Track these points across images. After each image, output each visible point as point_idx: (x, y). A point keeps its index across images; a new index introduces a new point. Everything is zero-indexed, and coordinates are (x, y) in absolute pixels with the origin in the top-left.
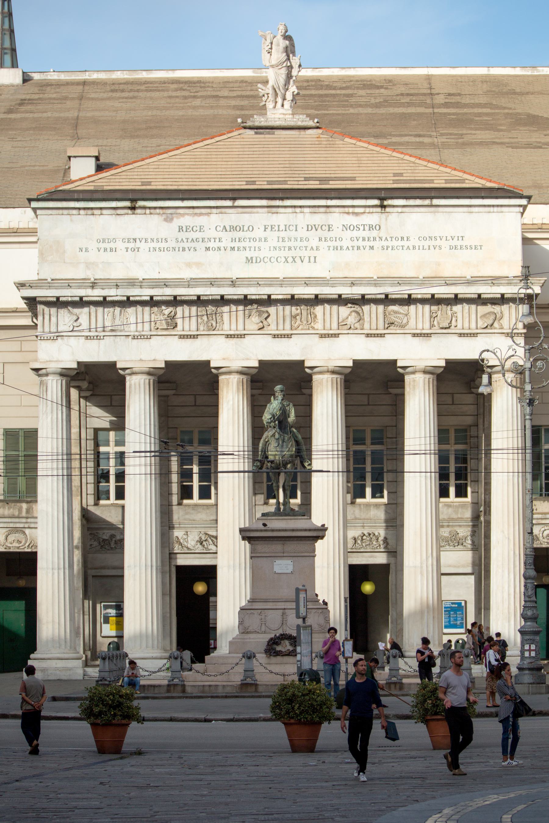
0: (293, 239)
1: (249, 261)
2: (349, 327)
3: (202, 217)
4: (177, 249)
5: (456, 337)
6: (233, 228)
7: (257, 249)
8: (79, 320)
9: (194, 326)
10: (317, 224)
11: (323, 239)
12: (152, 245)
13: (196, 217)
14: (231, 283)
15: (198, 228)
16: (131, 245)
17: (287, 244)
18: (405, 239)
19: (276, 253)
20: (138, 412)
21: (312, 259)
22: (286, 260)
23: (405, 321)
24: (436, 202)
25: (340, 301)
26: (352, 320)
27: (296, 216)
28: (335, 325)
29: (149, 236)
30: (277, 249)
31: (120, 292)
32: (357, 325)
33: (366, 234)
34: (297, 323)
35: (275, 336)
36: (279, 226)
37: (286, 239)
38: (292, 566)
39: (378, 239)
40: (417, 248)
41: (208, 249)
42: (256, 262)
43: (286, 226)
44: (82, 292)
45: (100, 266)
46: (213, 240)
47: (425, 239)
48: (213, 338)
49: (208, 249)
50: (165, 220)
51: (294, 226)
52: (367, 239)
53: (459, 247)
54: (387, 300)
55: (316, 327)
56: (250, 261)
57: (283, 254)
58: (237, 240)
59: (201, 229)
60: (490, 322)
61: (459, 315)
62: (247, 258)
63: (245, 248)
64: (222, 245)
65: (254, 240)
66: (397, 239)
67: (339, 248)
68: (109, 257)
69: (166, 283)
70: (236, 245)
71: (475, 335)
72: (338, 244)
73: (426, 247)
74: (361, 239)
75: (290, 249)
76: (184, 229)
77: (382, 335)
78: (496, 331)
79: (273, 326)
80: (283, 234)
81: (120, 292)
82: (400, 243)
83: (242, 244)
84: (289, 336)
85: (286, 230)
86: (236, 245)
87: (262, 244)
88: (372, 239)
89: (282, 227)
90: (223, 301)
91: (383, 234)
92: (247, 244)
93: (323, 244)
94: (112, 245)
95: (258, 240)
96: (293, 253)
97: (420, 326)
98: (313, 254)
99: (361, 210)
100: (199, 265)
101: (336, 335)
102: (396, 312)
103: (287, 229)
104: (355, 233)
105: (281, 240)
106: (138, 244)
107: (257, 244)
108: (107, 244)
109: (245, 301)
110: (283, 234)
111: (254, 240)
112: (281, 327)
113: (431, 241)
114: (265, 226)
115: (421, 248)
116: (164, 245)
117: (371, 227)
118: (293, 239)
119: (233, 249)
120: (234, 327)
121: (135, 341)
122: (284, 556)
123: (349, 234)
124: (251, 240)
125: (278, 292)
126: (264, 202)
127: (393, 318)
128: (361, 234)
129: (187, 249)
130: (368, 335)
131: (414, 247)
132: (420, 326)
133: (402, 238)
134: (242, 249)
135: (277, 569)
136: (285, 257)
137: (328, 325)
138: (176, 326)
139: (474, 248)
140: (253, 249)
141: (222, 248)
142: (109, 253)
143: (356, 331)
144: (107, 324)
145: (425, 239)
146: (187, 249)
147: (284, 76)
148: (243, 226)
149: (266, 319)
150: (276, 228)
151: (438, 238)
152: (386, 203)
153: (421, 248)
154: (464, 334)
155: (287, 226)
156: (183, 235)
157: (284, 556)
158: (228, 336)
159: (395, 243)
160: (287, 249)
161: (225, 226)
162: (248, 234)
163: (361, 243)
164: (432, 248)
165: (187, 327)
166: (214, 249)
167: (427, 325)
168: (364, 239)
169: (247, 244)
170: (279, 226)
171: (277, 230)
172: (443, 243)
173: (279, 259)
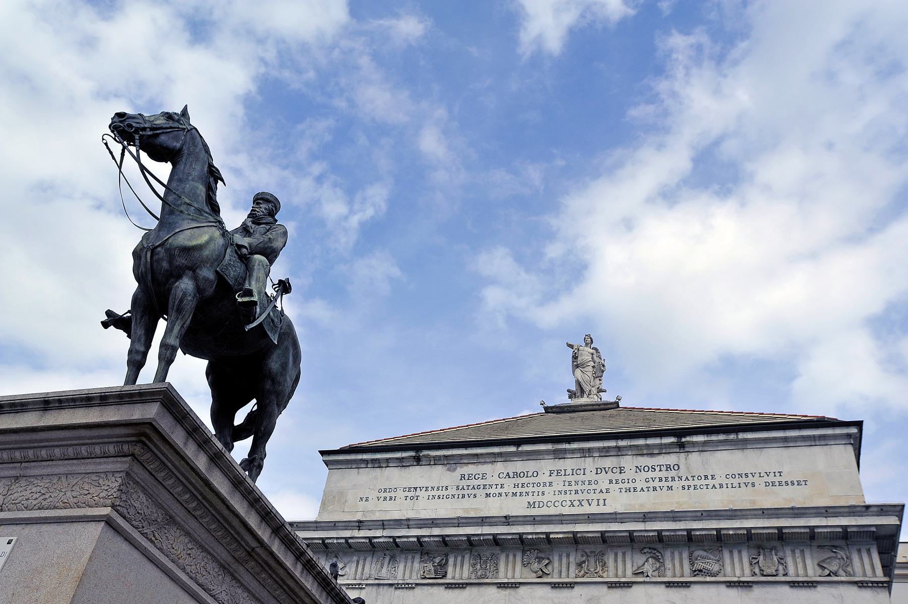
0: (580, 483)
2: (645, 574)
3: (486, 466)
4: (456, 496)
5: (786, 589)
6: (516, 475)
8: (347, 569)
9: (466, 574)
10: (607, 466)
11: (614, 482)
12: (433, 493)
13: (480, 466)
14: (504, 520)
15: (481, 476)
16: (410, 494)
17: (574, 488)
18: (710, 477)
21: (601, 502)
23: (716, 568)
24: (741, 436)
25: (632, 541)
26: (648, 568)
28: (629, 572)
29: (430, 485)
31: (387, 533)
32: (656, 573)
33: (664, 474)
34: (582, 572)
35: (555, 586)
37: (573, 483)
39: (676, 479)
40: (725, 486)
41: (488, 495)
44: (347, 534)
45: (377, 514)
46: (494, 487)
47: (733, 476)
48: (483, 589)
49: (488, 495)
50: (449, 470)
52: (664, 479)
53: (777, 484)
54: (690, 539)
55: (605, 575)
57: (568, 497)
58: (520, 485)
59: (484, 477)
60: (834, 568)
61: (790, 561)
64: (503, 491)
67: (632, 490)
68: (388, 505)
69: (433, 523)
70: (518, 490)
71: (811, 584)
72: (631, 485)
75: (577, 492)
76: (466, 477)
77: (686, 585)
78: (843, 579)
79: (556, 574)
81: (387, 533)
82: (704, 482)
84: (570, 585)
86: (518, 490)
87: (547, 489)
88: (670, 479)
89: (569, 472)
90: (496, 541)
91: (683, 472)
92: (530, 489)
93: (614, 486)
94: (393, 494)
96: (580, 496)
97: (738, 573)
98: (602, 496)
99: (656, 451)
100: (475, 509)
101: (628, 585)
104: (651, 474)
105: (567, 484)
106: (418, 492)
107: (541, 489)
108: (387, 494)
109: (523, 544)
112: (564, 574)
113: (744, 479)
115: (730, 486)
116: (445, 493)
117: (668, 468)
118: (580, 483)
119: (514, 494)
120: (510, 574)
121: (398, 592)
123: (644, 475)
125: (557, 530)
126: (549, 447)
127: (699, 565)
128: (657, 474)
129: (466, 496)
130: (669, 585)
131: (721, 486)
132: (738, 573)
133: (706, 477)
137: (620, 572)
138: (444, 576)
139: (796, 483)
141: (504, 494)
142: (388, 502)
143: (654, 580)
144: (373, 572)
145: (733, 476)
146: (466, 496)
147: (590, 374)
150: (563, 473)
151: (750, 475)
152: (684, 440)
153: (730, 486)
154: (798, 582)
156: (464, 483)
158: (501, 586)
159: (697, 482)
162: (532, 480)
163: (657, 484)
164: (742, 485)
165: (457, 576)
166: (494, 495)
167: (747, 571)
168: (661, 480)
169: (530, 489)
172: (756, 479)
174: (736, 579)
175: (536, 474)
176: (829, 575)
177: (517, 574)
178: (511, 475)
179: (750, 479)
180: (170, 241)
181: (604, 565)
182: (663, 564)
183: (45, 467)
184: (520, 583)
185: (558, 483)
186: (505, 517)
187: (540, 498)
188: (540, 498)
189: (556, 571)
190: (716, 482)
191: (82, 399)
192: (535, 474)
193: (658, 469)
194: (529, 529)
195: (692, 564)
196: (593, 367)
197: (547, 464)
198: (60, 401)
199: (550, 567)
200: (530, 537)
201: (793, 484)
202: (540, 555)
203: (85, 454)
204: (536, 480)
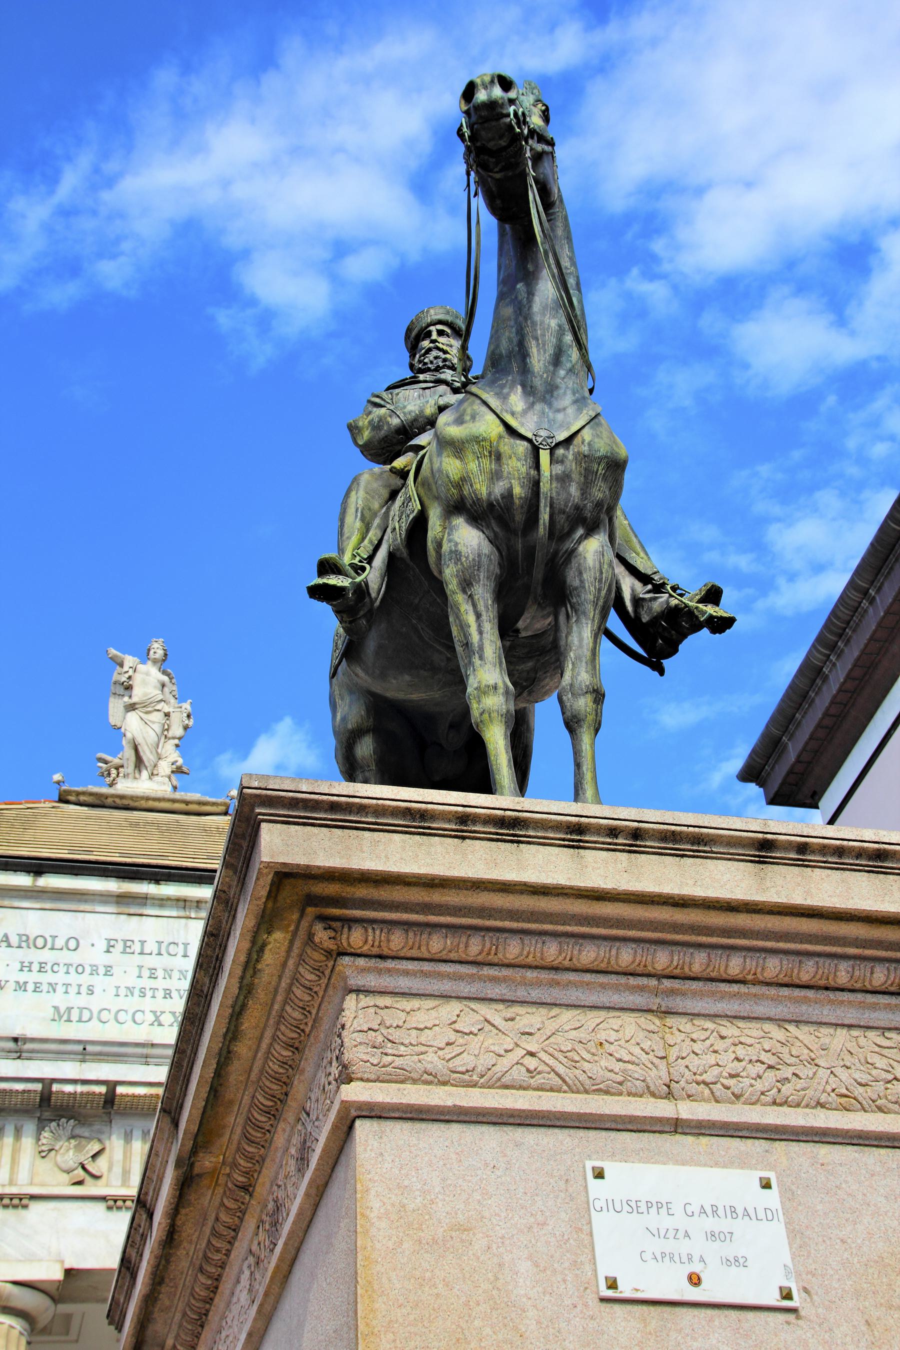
1: (61, 1017)
6: (26, 941)
7: (84, 990)
14: (11, 1045)
17: (161, 984)
19: (134, 1003)
22: (157, 1019)
27: (186, 925)
30: (137, 992)
36: (143, 942)
37: (160, 973)
38: (778, 1229)
42: (80, 1021)
43: (160, 943)
51: (181, 947)
56: (65, 1018)
57: (148, 1004)
58: (36, 967)
62: (56, 1008)
63: (53, 987)
65: (80, 969)
80: (152, 961)
83: (46, 978)
85: (160, 954)
87: (99, 981)
92: (60, 978)
95: (88, 969)
103: (163, 951)
105: (145, 973)
110: (152, 961)
111: (80, 969)
114: (109, 940)
119: (21, 986)
122: (677, 1126)
124: (72, 970)
126: (112, 885)
134: (45, 987)
135: (630, 1257)
136: (154, 1012)
140: (73, 990)
147: (157, 728)
148: (54, 937)
149: (94, 1157)
150: (137, 947)
155: (164, 946)
157: (677, 1126)
160: (161, 994)
161: (6, 936)
162: (65, 956)
169: (60, 978)
170: (143, 942)
171: (138, 950)
173: (139, 1017)
175: (74, 944)
177: (23, 1175)
178: (14, 940)
180: (587, 434)
183: (723, 996)
184: (33, 1197)
185: (127, 971)
186: (16, 1040)
187: (83, 1000)
188: (83, 1000)
189: (118, 1170)
191: (860, 853)
192: (73, 944)
194: (68, 1069)
196: (167, 715)
197: (99, 926)
198: (802, 848)
199: (102, 1161)
200: (69, 1088)
202: (78, 1131)
203: (843, 978)
204: (74, 958)
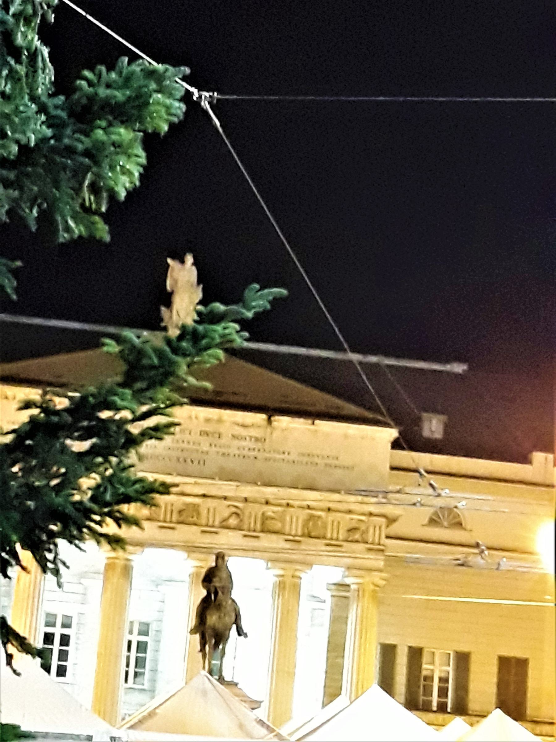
20: (27, 585)
24: (317, 422)
26: (233, 521)
28: (217, 523)
33: (252, 445)
39: (262, 450)
66: (279, 453)
73: (304, 462)
74: (247, 449)
82: (282, 456)
91: (267, 445)
93: (214, 449)
102: (273, 518)
104: (243, 443)
117: (257, 440)
123: (236, 443)
133: (284, 453)
145: (303, 455)
163: (246, 452)
174: (291, 538)
176: (351, 541)
179: (316, 460)
181: (199, 514)
182: (241, 521)
190: (291, 457)
193: (248, 438)
195: (263, 523)
201: (344, 467)
